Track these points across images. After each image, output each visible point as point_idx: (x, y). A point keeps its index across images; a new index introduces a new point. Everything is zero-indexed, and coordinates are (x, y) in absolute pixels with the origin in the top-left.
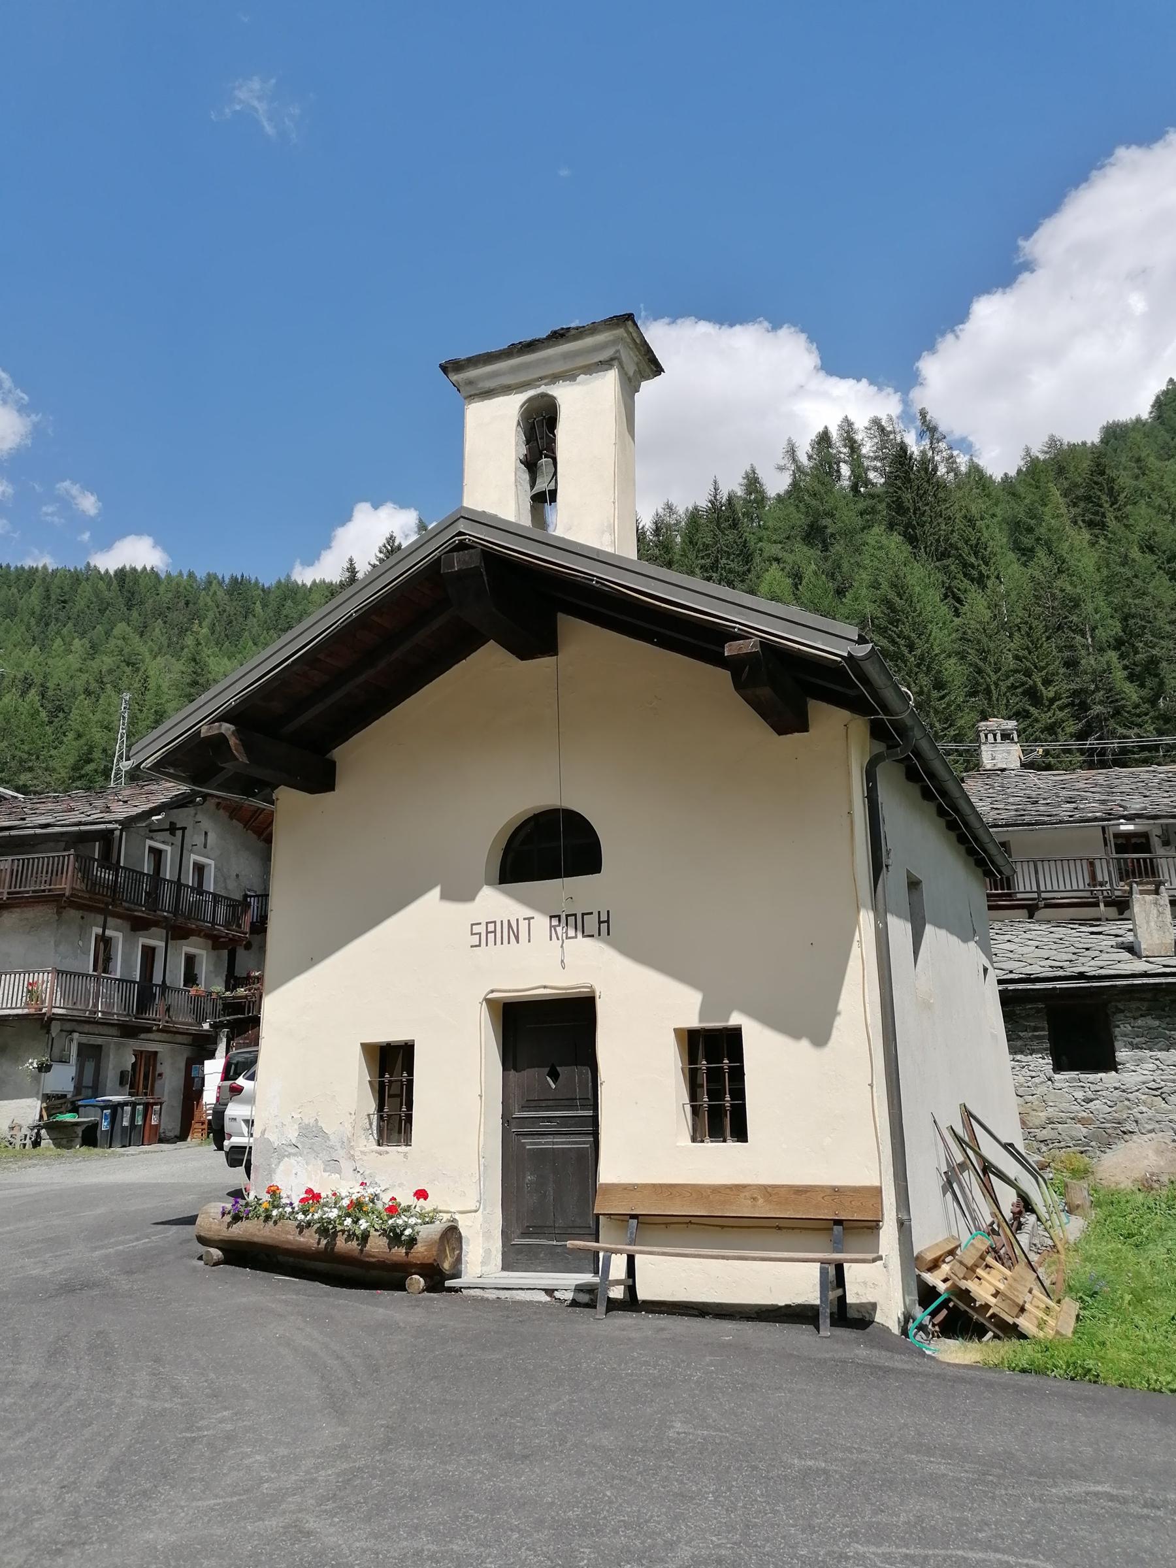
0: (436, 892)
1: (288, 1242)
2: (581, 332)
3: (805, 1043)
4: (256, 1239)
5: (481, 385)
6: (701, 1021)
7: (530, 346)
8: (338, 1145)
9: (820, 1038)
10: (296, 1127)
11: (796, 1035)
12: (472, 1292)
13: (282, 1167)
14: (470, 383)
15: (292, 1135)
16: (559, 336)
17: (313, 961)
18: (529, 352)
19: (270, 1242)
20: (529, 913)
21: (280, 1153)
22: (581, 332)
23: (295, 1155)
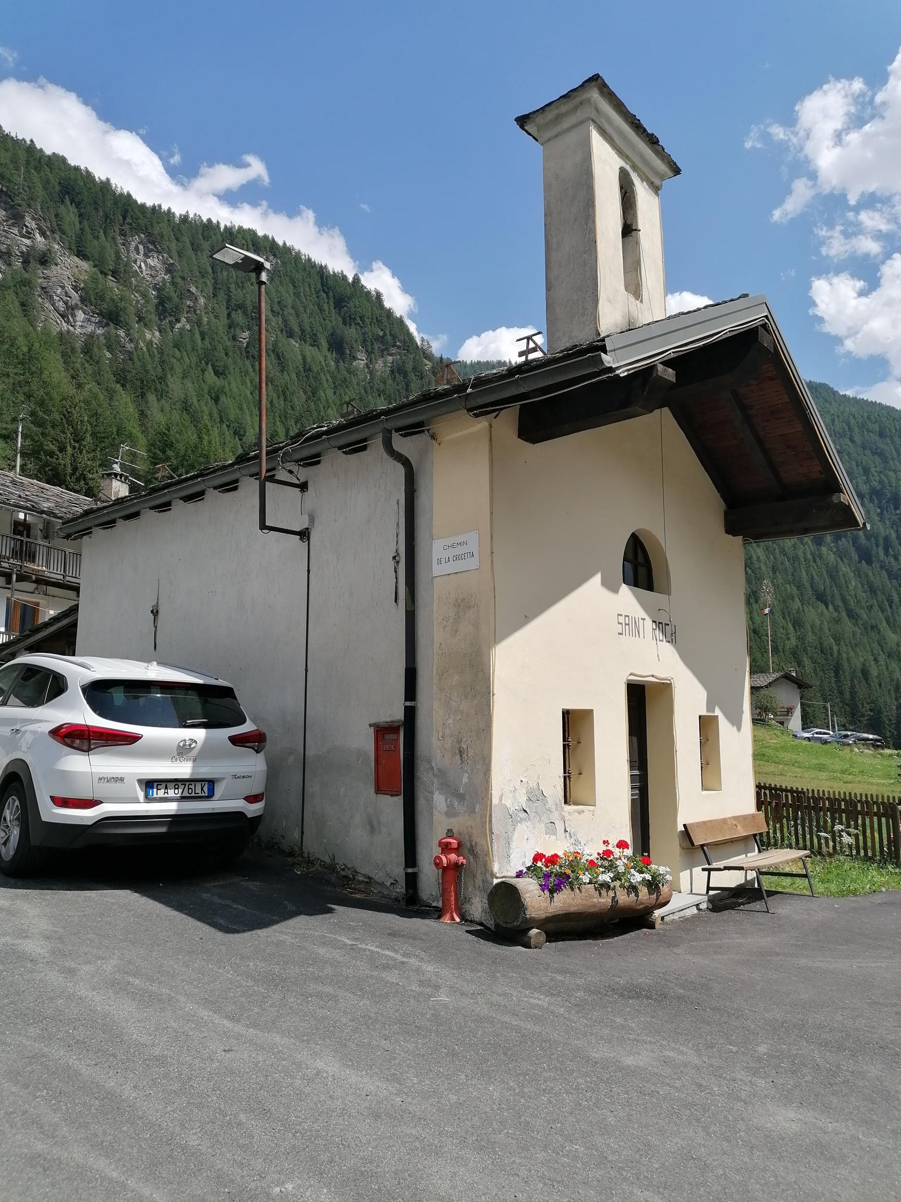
0: (597, 579)
1: (594, 906)
2: (661, 153)
3: (735, 728)
4: (572, 909)
5: (603, 120)
6: (708, 711)
7: (637, 126)
8: (554, 807)
9: (739, 729)
10: (524, 791)
11: (733, 725)
12: (671, 917)
13: (516, 834)
14: (597, 110)
15: (523, 800)
16: (652, 141)
17: (527, 619)
18: (631, 127)
19: (581, 909)
20: (645, 615)
21: (513, 819)
22: (661, 153)
23: (525, 820)
